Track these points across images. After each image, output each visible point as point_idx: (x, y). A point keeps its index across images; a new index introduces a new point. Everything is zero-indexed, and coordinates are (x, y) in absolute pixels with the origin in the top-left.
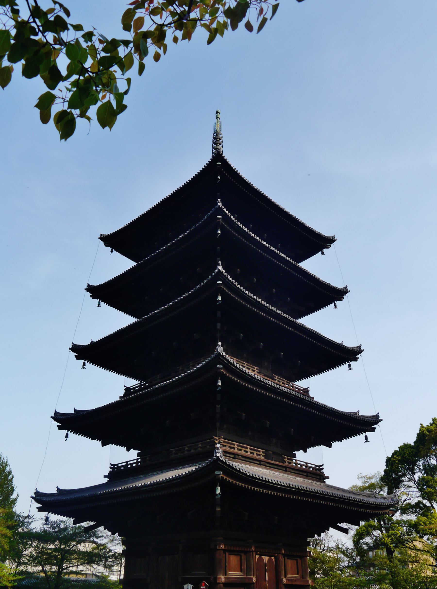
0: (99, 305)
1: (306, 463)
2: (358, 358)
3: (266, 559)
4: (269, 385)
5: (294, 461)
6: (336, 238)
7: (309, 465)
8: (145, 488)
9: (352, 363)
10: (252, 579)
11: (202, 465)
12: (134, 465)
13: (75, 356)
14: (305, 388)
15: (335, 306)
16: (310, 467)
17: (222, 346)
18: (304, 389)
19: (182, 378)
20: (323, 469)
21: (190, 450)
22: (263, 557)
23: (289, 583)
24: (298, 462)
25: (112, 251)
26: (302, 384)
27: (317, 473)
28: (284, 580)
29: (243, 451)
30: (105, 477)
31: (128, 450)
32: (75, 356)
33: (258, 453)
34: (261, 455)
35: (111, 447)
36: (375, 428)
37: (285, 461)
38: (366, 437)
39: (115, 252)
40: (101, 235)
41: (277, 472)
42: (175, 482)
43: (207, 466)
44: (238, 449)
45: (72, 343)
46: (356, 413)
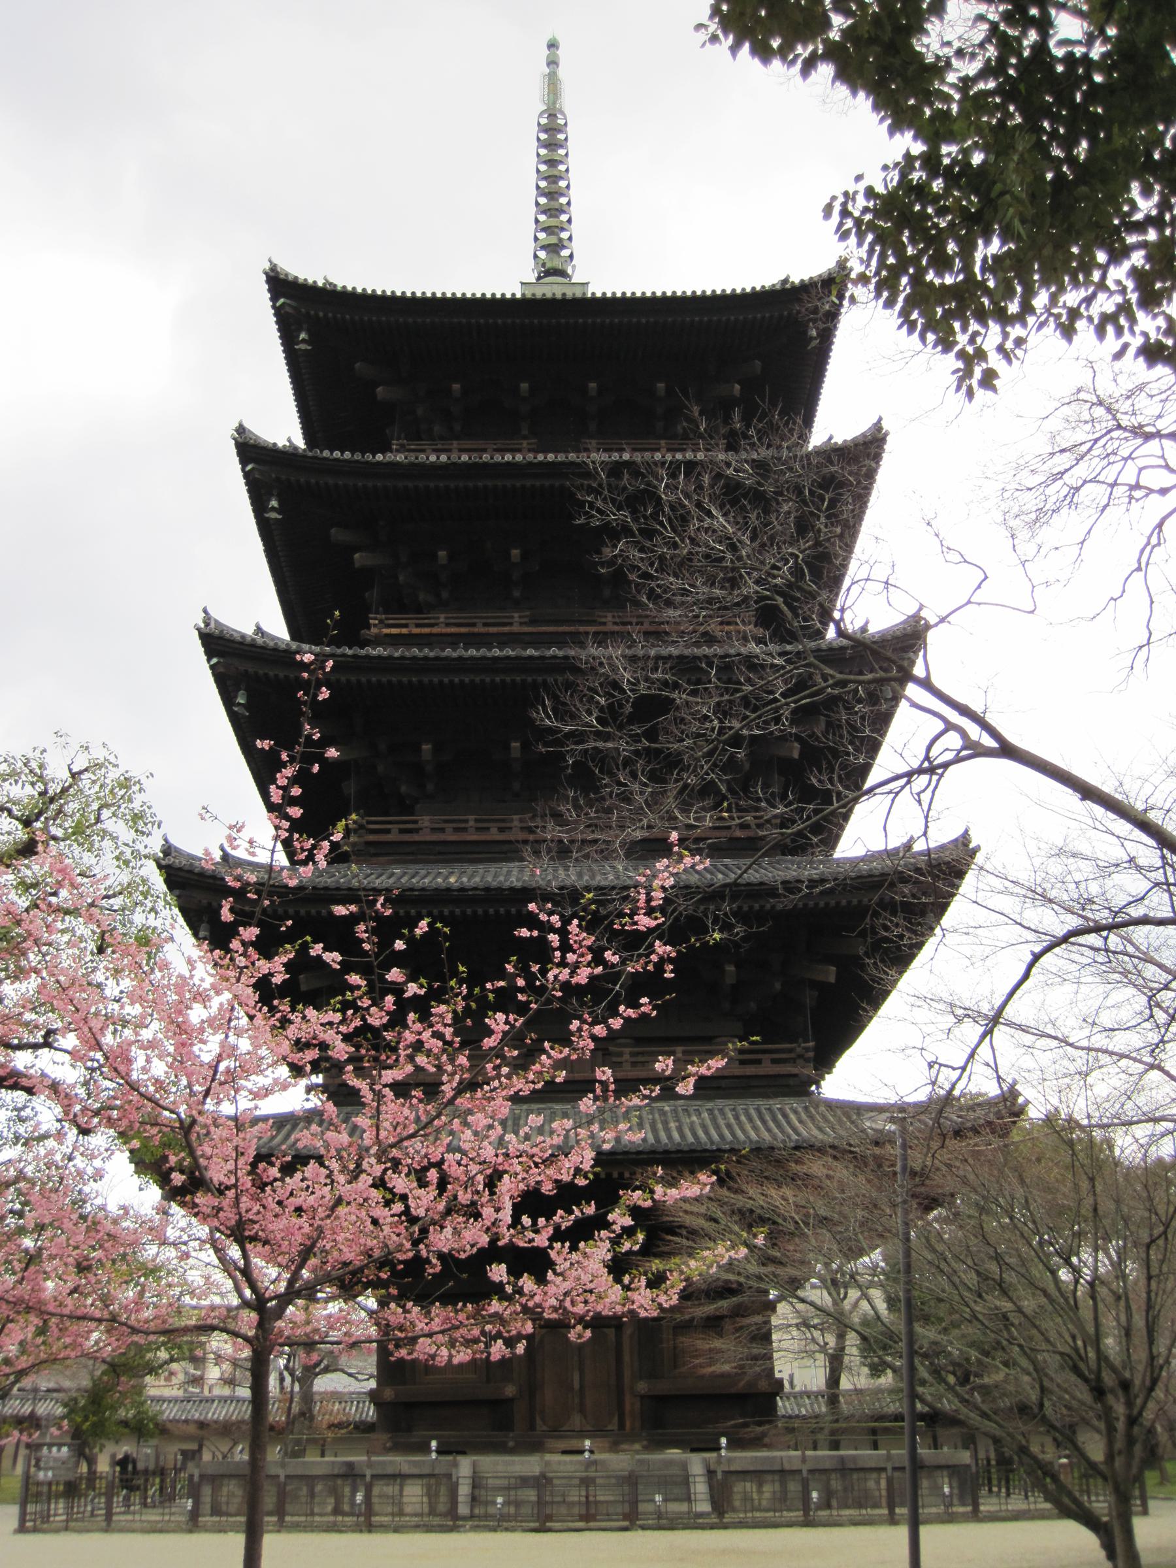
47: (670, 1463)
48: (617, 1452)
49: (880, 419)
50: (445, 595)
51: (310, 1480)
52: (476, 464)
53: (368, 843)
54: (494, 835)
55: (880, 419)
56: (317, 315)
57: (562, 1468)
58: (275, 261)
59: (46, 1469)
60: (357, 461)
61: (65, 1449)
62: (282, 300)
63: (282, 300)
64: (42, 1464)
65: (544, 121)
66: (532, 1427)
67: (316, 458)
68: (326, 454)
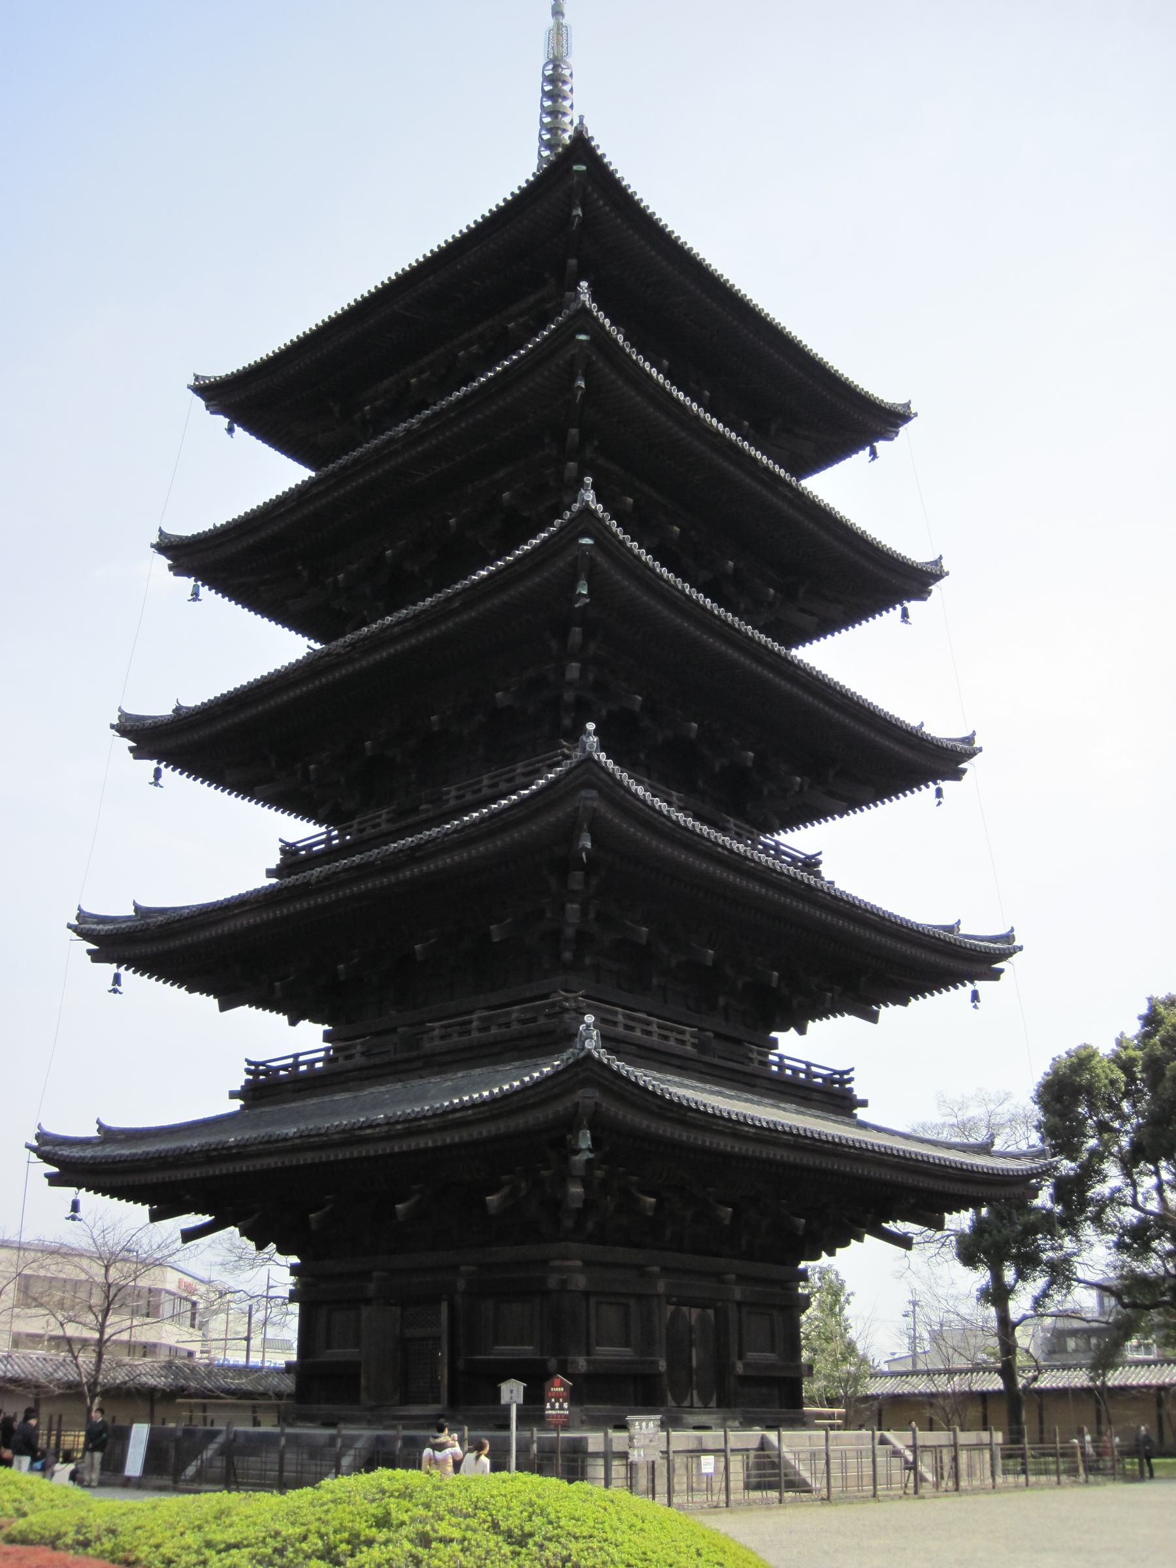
0: (195, 596)
1: (808, 1064)
2: (964, 771)
3: (694, 1314)
4: (724, 847)
5: (776, 1059)
6: (913, 410)
7: (814, 1069)
8: (369, 1131)
9: (946, 785)
10: (656, 1363)
11: (541, 1073)
12: (319, 1065)
13: (131, 749)
14: (810, 853)
15: (905, 615)
16: (817, 1075)
17: (596, 733)
18: (808, 857)
19: (473, 824)
20: (850, 1080)
21: (487, 1029)
22: (685, 1309)
23: (752, 1373)
24: (787, 1062)
25: (230, 430)
26: (799, 840)
27: (834, 1095)
28: (740, 1368)
29: (638, 1033)
30: (233, 1095)
31: (293, 1022)
33: (680, 1037)
34: (689, 1044)
35: (245, 1013)
36: (1002, 971)
37: (751, 1059)
38: (975, 996)
39: (238, 430)
40: (197, 378)
42: (458, 1115)
43: (557, 1074)
44: (627, 1027)
45: (120, 710)
46: (950, 929)
62: (584, 168)
63: (584, 168)
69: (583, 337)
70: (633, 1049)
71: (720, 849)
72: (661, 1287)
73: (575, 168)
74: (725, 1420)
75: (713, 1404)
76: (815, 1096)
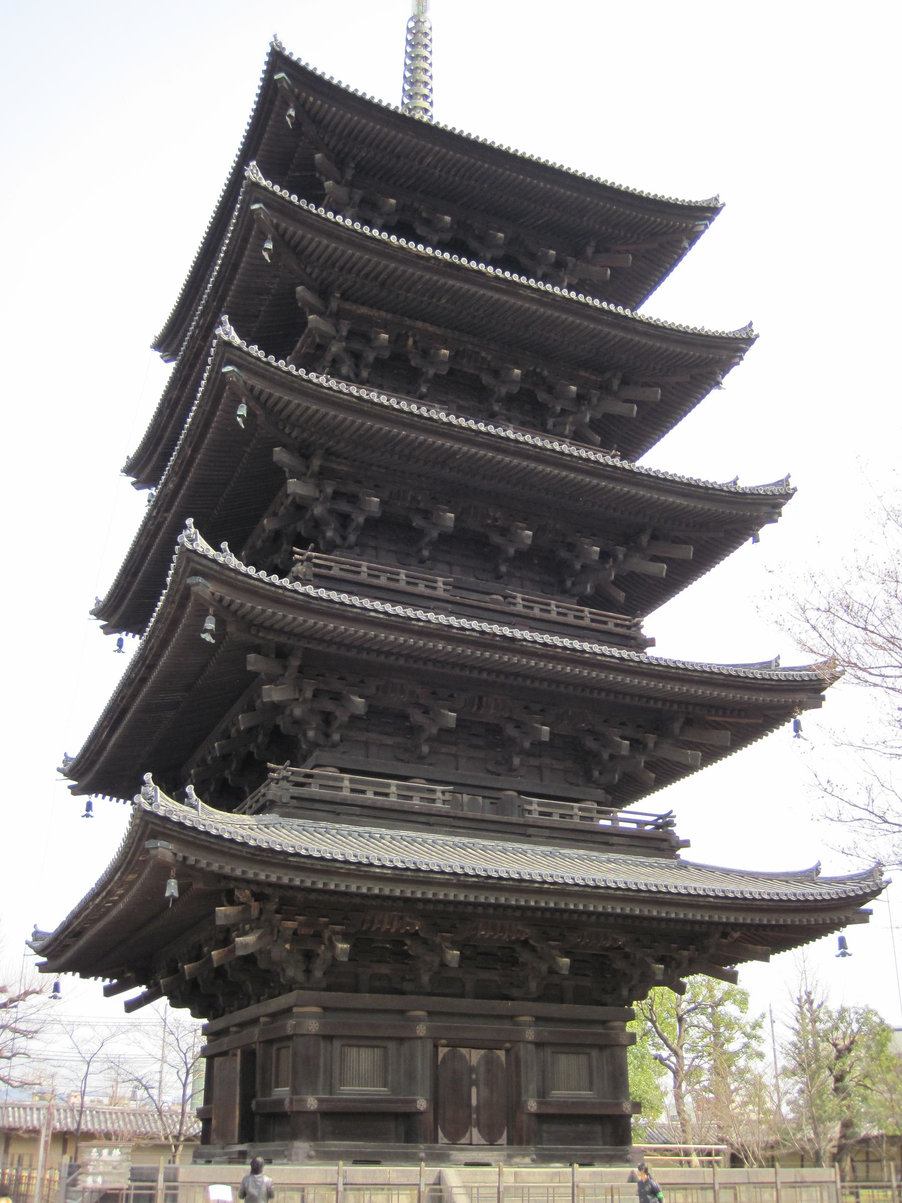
3: (475, 1056)
6: (721, 202)
13: (102, 627)
16: (647, 823)
22: (464, 1051)
28: (532, 1105)
29: (370, 795)
32: (102, 627)
41: (493, 839)
46: (766, 665)
47: (620, 1174)
48: (511, 1165)
49: (751, 324)
50: (365, 374)
51: (301, 1189)
52: (452, 265)
53: (316, 575)
54: (421, 589)
55: (751, 324)
56: (307, 98)
57: (531, 1178)
58: (279, 39)
59: (94, 1174)
60: (355, 231)
61: (117, 1152)
64: (90, 1169)
65: (412, 24)
66: (436, 1141)
67: (318, 215)
68: (330, 215)
69: (255, 207)
70: (358, 810)
71: (372, 614)
72: (421, 1030)
73: (276, 77)
74: (510, 1157)
75: (503, 1140)
76: (615, 840)
